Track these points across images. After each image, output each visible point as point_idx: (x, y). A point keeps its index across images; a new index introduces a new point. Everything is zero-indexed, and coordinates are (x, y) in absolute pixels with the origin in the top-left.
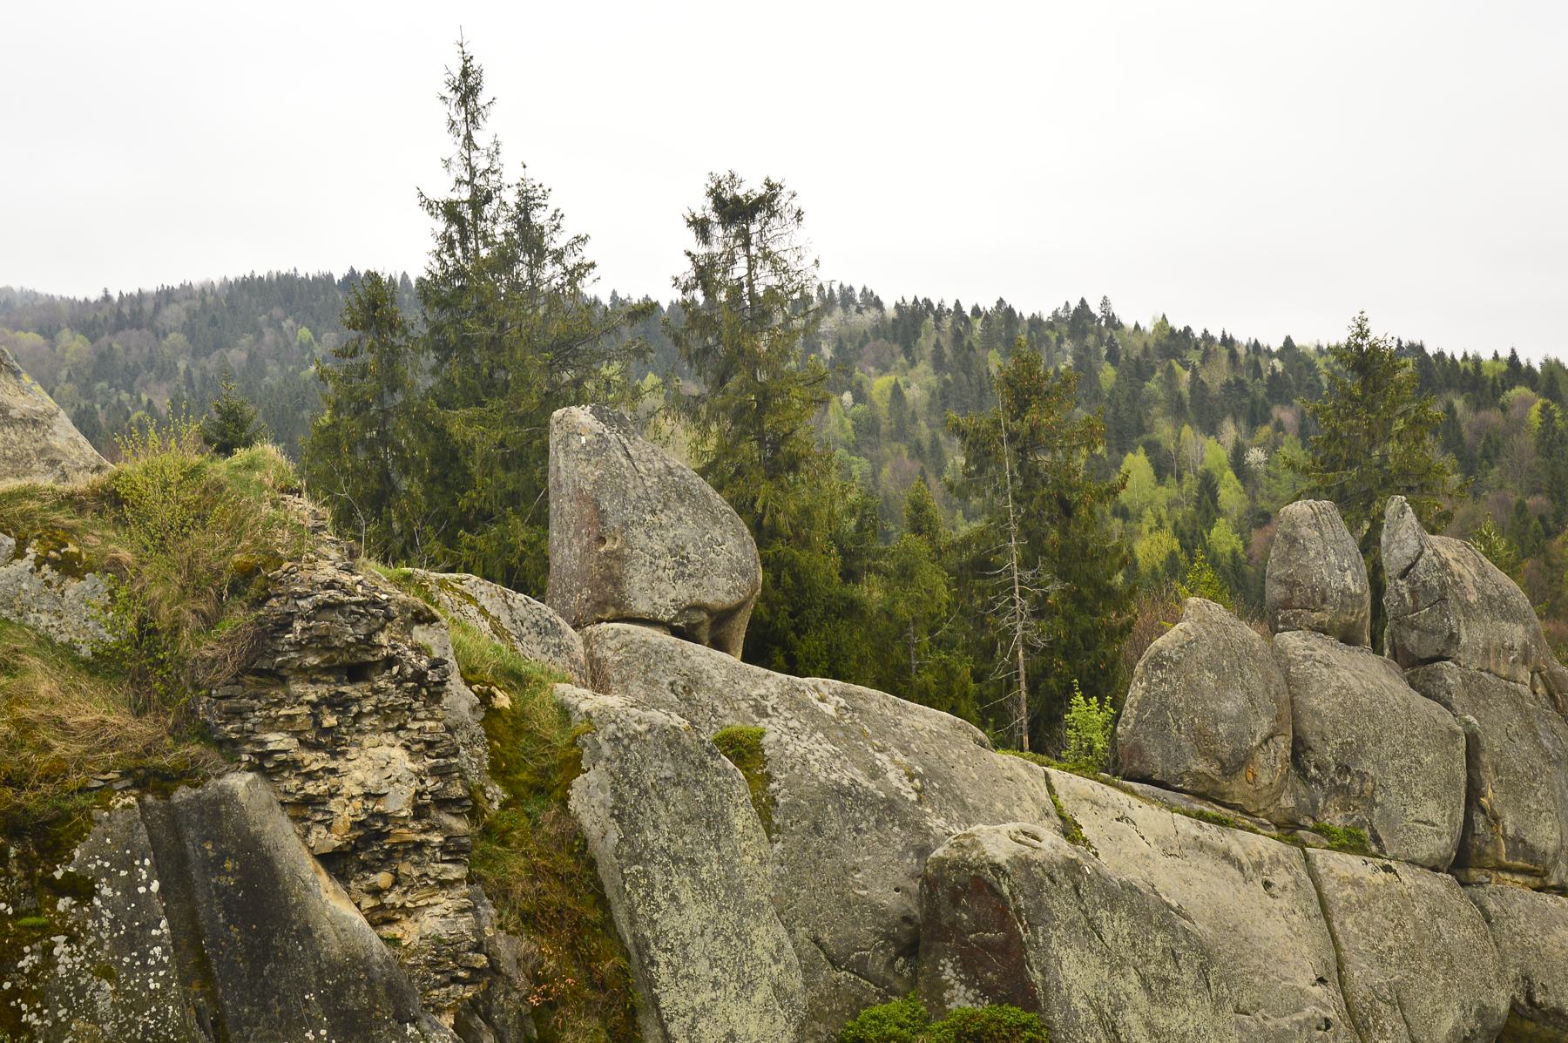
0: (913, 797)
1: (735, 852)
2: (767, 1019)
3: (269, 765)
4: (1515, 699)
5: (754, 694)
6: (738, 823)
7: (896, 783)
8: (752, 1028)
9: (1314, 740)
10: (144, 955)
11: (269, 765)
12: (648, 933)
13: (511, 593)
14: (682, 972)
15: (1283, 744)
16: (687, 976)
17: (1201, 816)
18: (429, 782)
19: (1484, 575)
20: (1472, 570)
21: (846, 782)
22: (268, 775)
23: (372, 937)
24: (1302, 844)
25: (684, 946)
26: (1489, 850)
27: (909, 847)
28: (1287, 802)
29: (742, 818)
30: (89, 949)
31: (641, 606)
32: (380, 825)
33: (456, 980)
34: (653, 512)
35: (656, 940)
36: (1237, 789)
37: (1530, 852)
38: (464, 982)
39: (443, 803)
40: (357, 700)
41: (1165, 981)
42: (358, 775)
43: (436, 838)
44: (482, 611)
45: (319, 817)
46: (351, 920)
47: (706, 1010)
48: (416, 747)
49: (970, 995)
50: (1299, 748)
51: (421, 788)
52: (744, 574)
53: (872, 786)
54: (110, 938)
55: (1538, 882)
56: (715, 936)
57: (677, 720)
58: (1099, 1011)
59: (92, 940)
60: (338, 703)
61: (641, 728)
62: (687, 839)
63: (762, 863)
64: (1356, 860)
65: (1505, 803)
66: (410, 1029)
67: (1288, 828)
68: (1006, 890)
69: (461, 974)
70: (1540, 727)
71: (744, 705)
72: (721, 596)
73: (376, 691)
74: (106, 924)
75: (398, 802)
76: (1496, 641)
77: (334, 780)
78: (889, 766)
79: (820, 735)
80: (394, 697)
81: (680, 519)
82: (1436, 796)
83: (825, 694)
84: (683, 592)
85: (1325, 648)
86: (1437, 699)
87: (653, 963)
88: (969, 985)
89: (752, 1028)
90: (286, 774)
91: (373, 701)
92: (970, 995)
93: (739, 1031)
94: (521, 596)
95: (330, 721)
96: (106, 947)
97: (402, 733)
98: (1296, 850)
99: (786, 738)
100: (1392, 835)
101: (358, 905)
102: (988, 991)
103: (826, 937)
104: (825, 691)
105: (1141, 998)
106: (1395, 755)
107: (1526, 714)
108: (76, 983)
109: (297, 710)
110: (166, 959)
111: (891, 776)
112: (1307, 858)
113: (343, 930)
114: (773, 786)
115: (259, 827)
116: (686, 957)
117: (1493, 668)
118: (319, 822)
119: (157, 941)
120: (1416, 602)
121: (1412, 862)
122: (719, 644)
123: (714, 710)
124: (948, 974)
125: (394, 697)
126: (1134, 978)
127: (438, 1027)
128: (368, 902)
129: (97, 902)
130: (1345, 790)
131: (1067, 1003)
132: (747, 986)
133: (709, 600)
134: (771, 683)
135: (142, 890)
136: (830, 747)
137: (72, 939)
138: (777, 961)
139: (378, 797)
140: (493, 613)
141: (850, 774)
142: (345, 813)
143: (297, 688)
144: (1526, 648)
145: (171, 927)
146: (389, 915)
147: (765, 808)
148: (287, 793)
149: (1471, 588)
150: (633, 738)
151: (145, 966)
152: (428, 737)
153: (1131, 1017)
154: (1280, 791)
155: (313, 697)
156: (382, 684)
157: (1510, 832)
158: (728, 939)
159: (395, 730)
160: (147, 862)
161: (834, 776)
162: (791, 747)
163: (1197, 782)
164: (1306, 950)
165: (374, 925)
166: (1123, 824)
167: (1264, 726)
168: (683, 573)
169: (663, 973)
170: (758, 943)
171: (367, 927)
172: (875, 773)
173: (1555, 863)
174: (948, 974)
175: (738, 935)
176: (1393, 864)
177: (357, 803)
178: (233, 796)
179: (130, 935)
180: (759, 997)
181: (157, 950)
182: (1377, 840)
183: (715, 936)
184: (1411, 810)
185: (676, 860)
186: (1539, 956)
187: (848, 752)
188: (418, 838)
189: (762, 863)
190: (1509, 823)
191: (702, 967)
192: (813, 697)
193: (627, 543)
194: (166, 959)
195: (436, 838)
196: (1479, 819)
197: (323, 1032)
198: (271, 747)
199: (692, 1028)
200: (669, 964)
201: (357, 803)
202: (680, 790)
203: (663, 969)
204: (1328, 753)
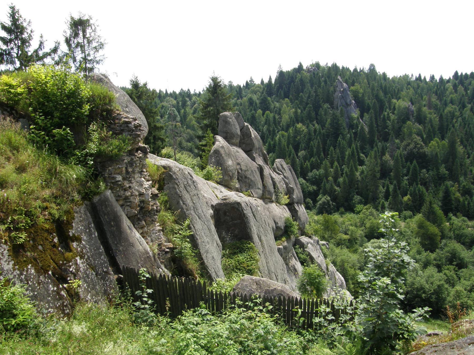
9: (240, 171)
16: (203, 242)
30: (86, 260)
50: (238, 172)
58: (258, 237)
68: (241, 209)
74: (88, 250)
87: (197, 239)
90: (118, 190)
105: (263, 232)
108: (86, 274)
110: (105, 259)
118: (127, 206)
120: (244, 137)
128: (141, 231)
130: (245, 182)
137: (81, 258)
148: (119, 196)
182: (252, 193)
194: (105, 259)
199: (207, 257)
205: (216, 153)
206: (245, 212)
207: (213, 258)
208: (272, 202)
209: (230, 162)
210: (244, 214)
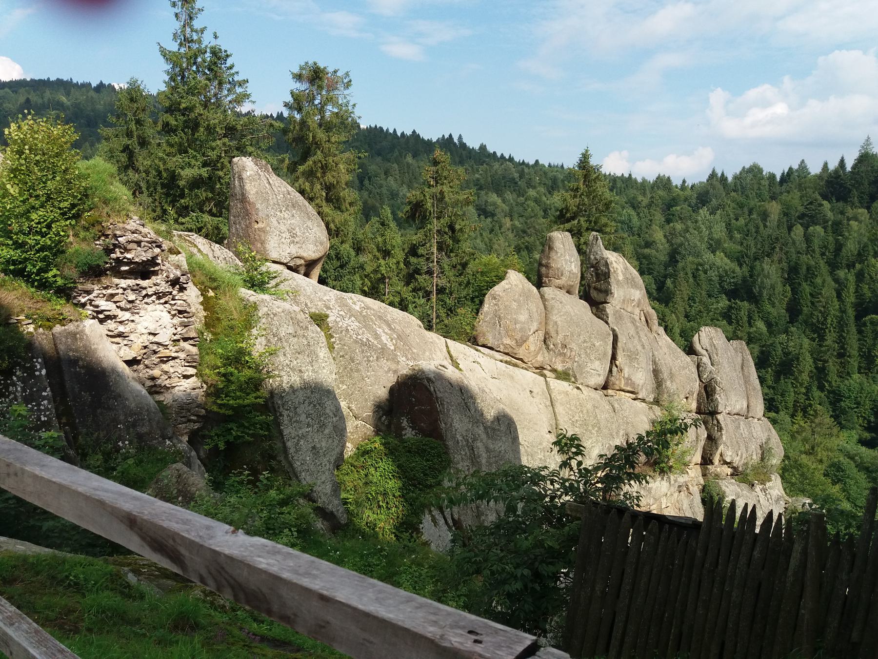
0: (392, 348)
1: (319, 367)
2: (330, 441)
3: (101, 316)
4: (633, 322)
5: (325, 298)
6: (321, 355)
7: (385, 342)
8: (324, 444)
9: (553, 334)
10: (39, 405)
11: (101, 316)
12: (279, 402)
13: (213, 244)
14: (294, 419)
15: (541, 335)
17: (506, 362)
18: (179, 329)
19: (626, 269)
21: (365, 340)
22: (101, 321)
23: (150, 400)
24: (545, 376)
25: (296, 408)
26: (617, 382)
27: (389, 370)
28: (540, 358)
29: (323, 353)
31: (274, 255)
32: (155, 347)
33: (190, 421)
34: (281, 211)
35: (283, 405)
36: (521, 352)
37: (633, 384)
38: (194, 422)
39: (185, 339)
40: (145, 288)
41: (494, 429)
42: (146, 324)
43: (182, 355)
44: (199, 250)
45: (125, 342)
46: (140, 392)
47: (303, 436)
48: (173, 312)
49: (413, 433)
51: (175, 331)
52: (321, 244)
53: (376, 342)
54: (22, 395)
55: (634, 396)
56: (310, 403)
57: (297, 309)
59: (12, 396)
60: (137, 289)
61: (280, 310)
62: (299, 361)
63: (331, 373)
64: (565, 384)
65: (626, 364)
66: (168, 442)
67: (540, 369)
68: (432, 389)
69: (193, 418)
70: (642, 334)
71: (319, 303)
72: (311, 253)
73: (155, 285)
74: (19, 389)
75: (165, 337)
76: (628, 297)
77: (132, 324)
78: (383, 334)
79: (353, 318)
80: (164, 287)
81: (293, 216)
82: (600, 359)
83: (357, 301)
84: (294, 250)
85: (561, 295)
86: (602, 319)
87: (281, 415)
88: (413, 428)
89: (324, 444)
91: (154, 289)
92: (413, 433)
93: (318, 446)
94: (218, 245)
95: (132, 297)
96: (20, 400)
97: (166, 305)
98: (542, 378)
99: (338, 319)
100: (581, 374)
101: (143, 385)
102: (421, 431)
103: (353, 407)
104: (355, 300)
106: (585, 341)
107: (637, 328)
109: (117, 291)
111: (383, 338)
112: (546, 381)
113: (137, 396)
114: (333, 340)
115: (96, 346)
116: (296, 413)
119: (44, 398)
121: (588, 386)
122: (307, 275)
123: (306, 305)
124: (405, 423)
125: (164, 287)
126: (482, 428)
127: (181, 442)
128: (149, 383)
129: (15, 378)
131: (454, 437)
132: (323, 426)
133: (305, 255)
134: (330, 295)
135: (37, 373)
136: (357, 324)
138: (336, 416)
139: (155, 335)
140: (205, 252)
141: (366, 336)
142: (139, 340)
143: (116, 281)
144: (639, 300)
145: (52, 390)
146: (158, 389)
147: (331, 347)
149: (620, 274)
150: (275, 315)
151: (39, 410)
152: (179, 308)
153: (479, 444)
154: (538, 353)
155: (124, 286)
156: (158, 281)
157: (626, 376)
158: (315, 406)
159: (163, 304)
160: (40, 360)
161: (359, 337)
162: (341, 323)
163: (506, 348)
164: (545, 419)
165: (151, 393)
166: (476, 364)
167: (535, 326)
168: (293, 242)
169: (285, 420)
170: (328, 408)
171: (148, 395)
172: (377, 337)
173: (642, 389)
174: (405, 423)
175: (319, 404)
176: (580, 386)
177: (145, 337)
178: (83, 331)
179: (31, 394)
180: (327, 431)
181: (46, 402)
182: (575, 377)
183: (310, 403)
184: (589, 364)
185: (293, 369)
186: (633, 426)
187: (365, 327)
188: (174, 355)
189: (331, 373)
190: (626, 372)
191: (303, 417)
192: (350, 302)
193: (268, 225)
195: (182, 355)
196: (615, 369)
197: (127, 442)
198: (102, 308)
200: (288, 416)
201: (145, 337)
202: (296, 339)
203: (285, 418)
204: (559, 339)
205: (495, 299)
206: (439, 395)
207: (314, 448)
208: (643, 400)
209: (523, 317)
210: (437, 398)
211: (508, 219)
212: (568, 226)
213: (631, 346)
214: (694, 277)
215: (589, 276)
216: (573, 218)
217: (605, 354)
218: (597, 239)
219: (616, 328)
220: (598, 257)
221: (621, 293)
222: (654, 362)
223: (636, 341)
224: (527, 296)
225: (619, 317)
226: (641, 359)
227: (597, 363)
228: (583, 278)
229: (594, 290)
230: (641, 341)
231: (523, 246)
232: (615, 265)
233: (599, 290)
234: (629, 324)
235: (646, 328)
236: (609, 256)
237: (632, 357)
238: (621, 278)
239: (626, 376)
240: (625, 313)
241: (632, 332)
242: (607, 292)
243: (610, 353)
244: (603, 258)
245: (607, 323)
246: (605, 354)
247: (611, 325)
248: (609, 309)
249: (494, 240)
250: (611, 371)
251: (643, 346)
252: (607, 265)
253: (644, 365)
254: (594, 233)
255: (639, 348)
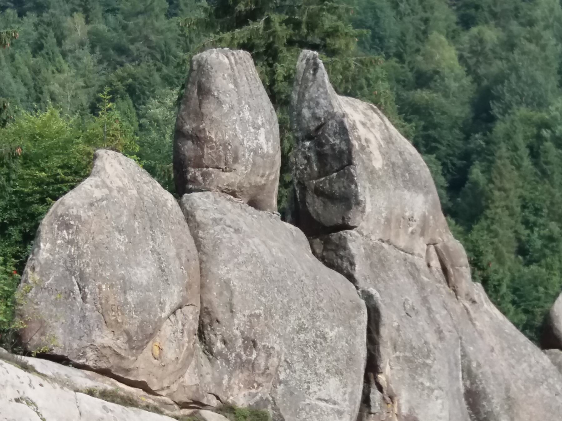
4: (413, 273)
20: (378, 135)
70: (435, 303)
76: (397, 211)
86: (339, 270)
107: (422, 287)
117: (393, 240)
144: (425, 219)
149: (376, 154)
211: (79, 18)
212: (241, 34)
213: (409, 334)
214: (534, 154)
215: (301, 160)
216: (253, 15)
217: (351, 359)
218: (316, 68)
219: (373, 291)
220: (320, 112)
221: (382, 203)
222: (468, 373)
223: (422, 322)
224: (151, 217)
225: (379, 264)
226: (436, 366)
227: (333, 382)
228: (285, 167)
229: (316, 198)
230: (433, 320)
231: (120, 86)
232: (362, 131)
233: (329, 197)
234: (404, 280)
235: (443, 287)
236: (348, 110)
237: (416, 362)
238: (378, 163)
239: (404, 411)
240: (393, 252)
241: (412, 298)
242: (348, 200)
243: (363, 353)
244: (333, 116)
245: (351, 278)
246: (351, 359)
247: (362, 284)
248: (355, 243)
249: (46, 73)
250: (366, 401)
251: (439, 332)
252: (343, 131)
253: (444, 381)
254: (308, 53)
255: (431, 338)
